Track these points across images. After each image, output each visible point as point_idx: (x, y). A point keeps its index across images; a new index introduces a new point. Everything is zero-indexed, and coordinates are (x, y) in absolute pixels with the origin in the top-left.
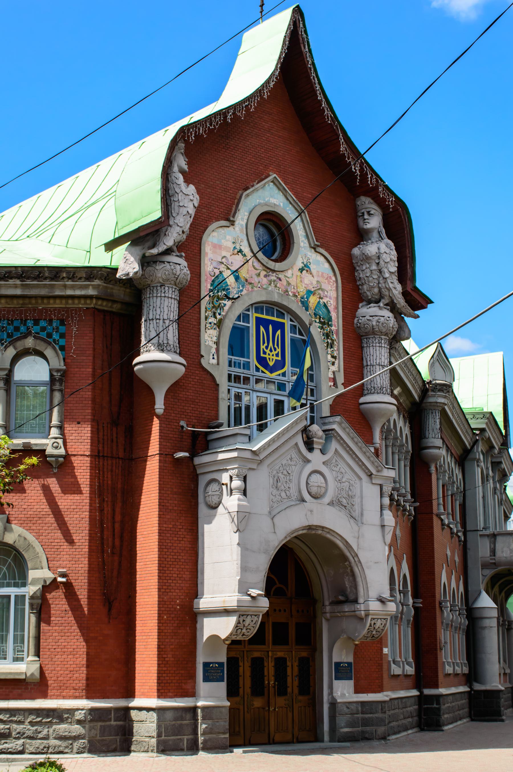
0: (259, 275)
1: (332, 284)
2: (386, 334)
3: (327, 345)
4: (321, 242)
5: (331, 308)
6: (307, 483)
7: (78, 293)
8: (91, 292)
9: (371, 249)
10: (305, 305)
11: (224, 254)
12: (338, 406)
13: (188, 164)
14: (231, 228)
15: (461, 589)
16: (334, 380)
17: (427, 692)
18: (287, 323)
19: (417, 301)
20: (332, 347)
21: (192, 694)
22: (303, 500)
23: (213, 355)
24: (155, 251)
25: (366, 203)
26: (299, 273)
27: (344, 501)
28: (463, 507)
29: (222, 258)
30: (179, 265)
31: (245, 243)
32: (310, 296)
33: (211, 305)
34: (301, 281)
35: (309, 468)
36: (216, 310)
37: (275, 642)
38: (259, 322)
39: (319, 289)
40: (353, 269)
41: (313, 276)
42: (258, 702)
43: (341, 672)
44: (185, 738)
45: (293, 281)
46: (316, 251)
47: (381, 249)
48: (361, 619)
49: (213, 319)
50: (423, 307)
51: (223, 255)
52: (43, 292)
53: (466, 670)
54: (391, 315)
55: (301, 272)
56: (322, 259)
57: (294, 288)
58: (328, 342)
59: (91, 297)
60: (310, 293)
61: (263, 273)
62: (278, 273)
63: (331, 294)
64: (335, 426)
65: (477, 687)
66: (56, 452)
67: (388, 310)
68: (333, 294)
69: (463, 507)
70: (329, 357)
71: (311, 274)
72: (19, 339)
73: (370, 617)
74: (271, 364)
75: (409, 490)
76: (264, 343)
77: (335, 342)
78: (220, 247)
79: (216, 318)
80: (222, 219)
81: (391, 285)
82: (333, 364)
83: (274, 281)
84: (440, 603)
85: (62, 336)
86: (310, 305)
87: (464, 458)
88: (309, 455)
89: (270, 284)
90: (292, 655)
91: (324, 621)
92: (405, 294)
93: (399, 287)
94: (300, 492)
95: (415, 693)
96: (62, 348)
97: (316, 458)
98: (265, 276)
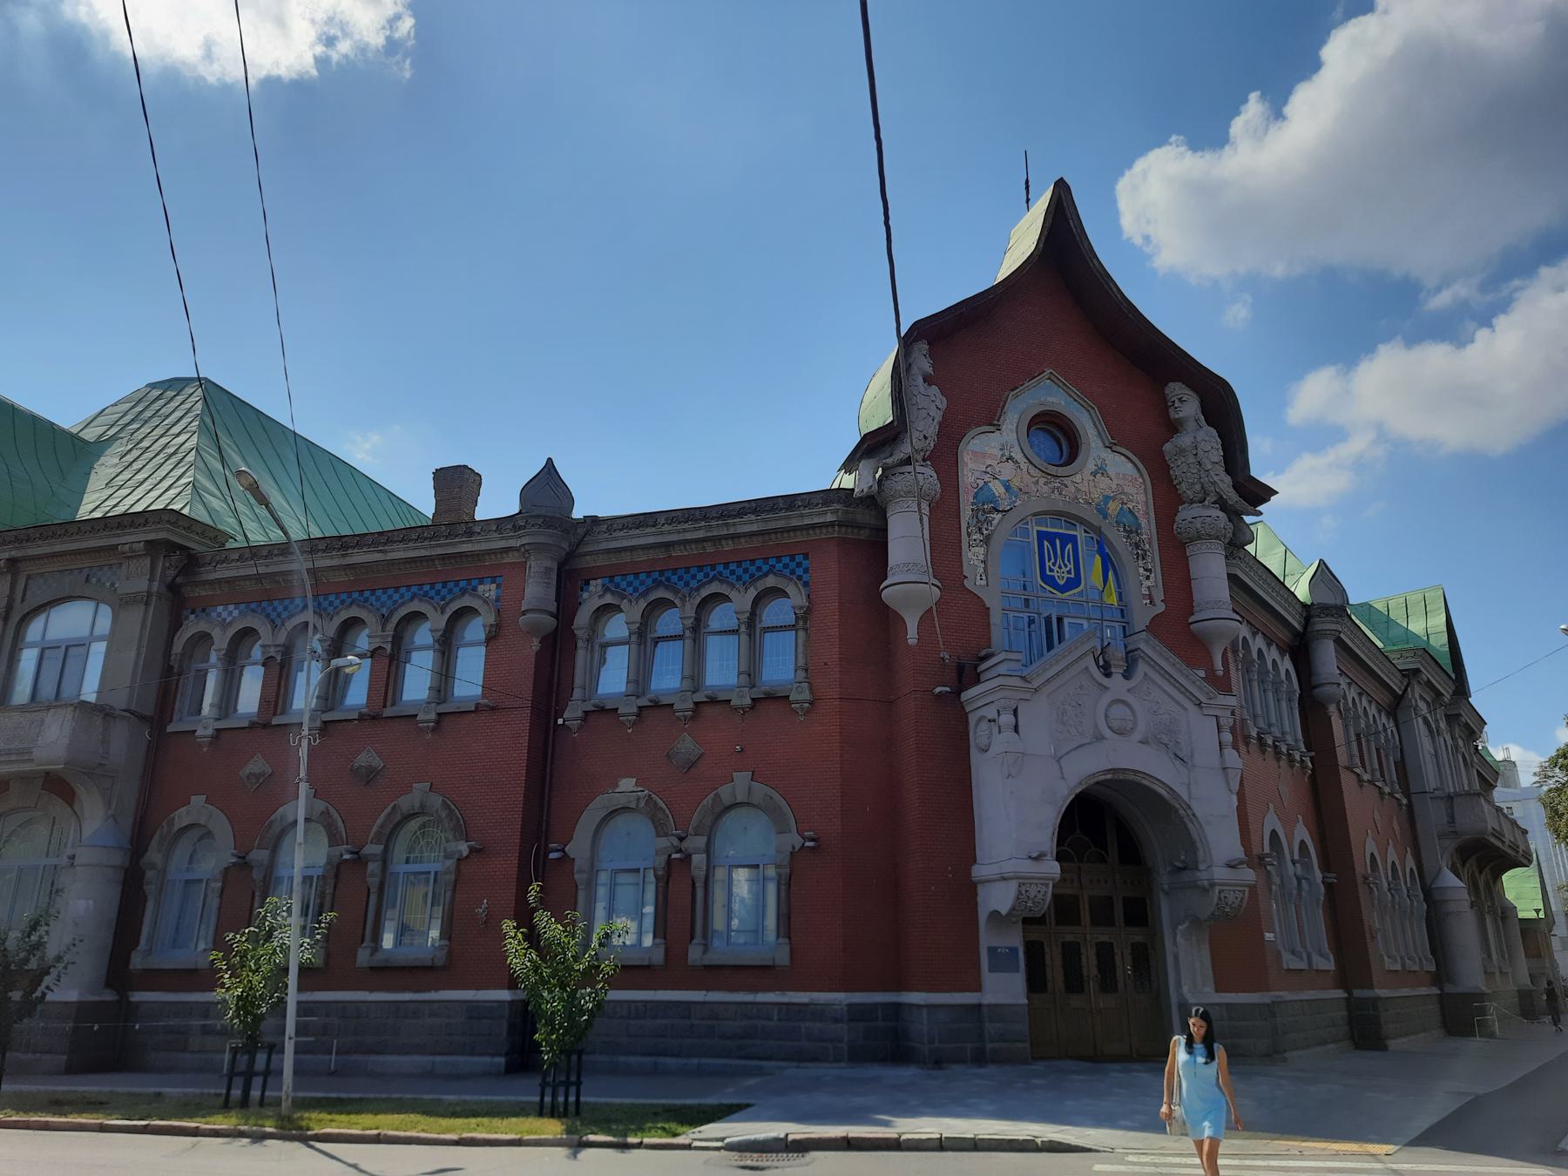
2: (1217, 538)
4: (1117, 439)
6: (1106, 716)
7: (816, 520)
8: (829, 518)
9: (1184, 440)
12: (1155, 627)
13: (933, 366)
15: (1410, 863)
16: (1150, 596)
17: (1357, 993)
18: (1079, 533)
19: (1258, 494)
21: (978, 988)
22: (1103, 738)
24: (889, 461)
25: (1176, 389)
27: (1165, 739)
28: (1401, 766)
30: (927, 476)
31: (1017, 448)
35: (1107, 698)
37: (1094, 922)
38: (1042, 536)
40: (1166, 468)
42: (1076, 1001)
44: (969, 1046)
47: (1198, 441)
48: (1205, 890)
50: (1265, 500)
52: (781, 524)
53: (1433, 969)
54: (1221, 514)
59: (832, 524)
60: (1107, 499)
61: (1042, 481)
64: (1142, 646)
66: (800, 697)
68: (1141, 498)
69: (1401, 766)
71: (1110, 476)
72: (760, 578)
73: (1217, 889)
74: (1062, 582)
75: (1300, 736)
78: (984, 455)
82: (1148, 578)
84: (1366, 878)
85: (806, 571)
87: (1395, 706)
88: (1105, 681)
90: (1123, 939)
91: (1162, 896)
93: (1228, 479)
94: (1096, 726)
95: (1340, 994)
96: (806, 584)
97: (1117, 683)
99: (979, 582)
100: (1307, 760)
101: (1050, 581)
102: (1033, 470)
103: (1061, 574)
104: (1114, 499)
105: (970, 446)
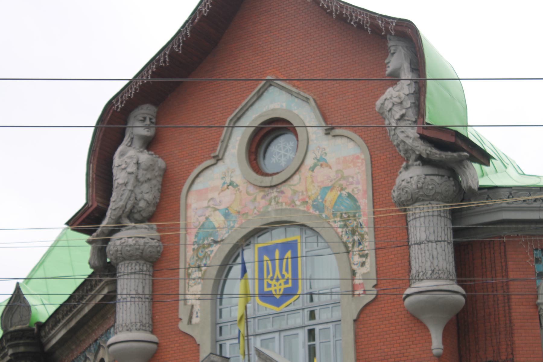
0: (255, 199)
1: (360, 164)
3: (353, 245)
5: (359, 196)
10: (319, 207)
11: (210, 196)
14: (220, 163)
20: (360, 244)
23: (197, 313)
26: (310, 173)
29: (209, 201)
31: (238, 172)
32: (326, 194)
33: (196, 258)
34: (313, 182)
36: (201, 261)
39: (340, 180)
41: (331, 168)
45: (300, 188)
46: (334, 136)
49: (197, 273)
51: (210, 197)
55: (313, 171)
56: (345, 140)
57: (302, 195)
58: (354, 241)
60: (325, 189)
62: (279, 187)
67: (419, 165)
70: (356, 259)
76: (268, 273)
77: (366, 236)
79: (201, 271)
80: (206, 159)
81: (402, 136)
82: (363, 264)
83: (275, 197)
86: (327, 204)
89: (270, 204)
92: (423, 138)
98: (263, 197)
99: (195, 320)
101: (267, 297)
102: (251, 189)
103: (277, 288)
104: (332, 188)
105: (195, 187)
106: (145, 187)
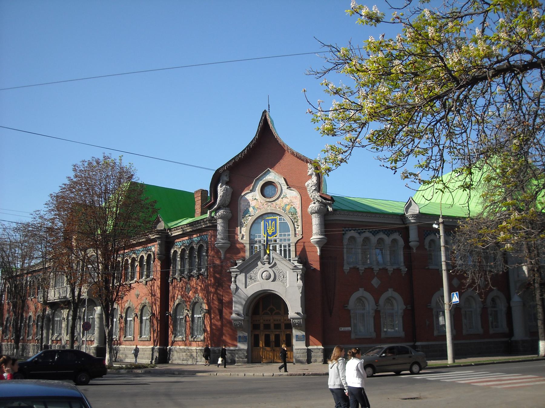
25: (309, 166)
31: (258, 195)
35: (262, 270)
43: (298, 338)
63: (297, 204)
65: (513, 339)
71: (290, 197)
95: (412, 344)
100: (404, 269)
104: (288, 205)
106: (228, 197)
